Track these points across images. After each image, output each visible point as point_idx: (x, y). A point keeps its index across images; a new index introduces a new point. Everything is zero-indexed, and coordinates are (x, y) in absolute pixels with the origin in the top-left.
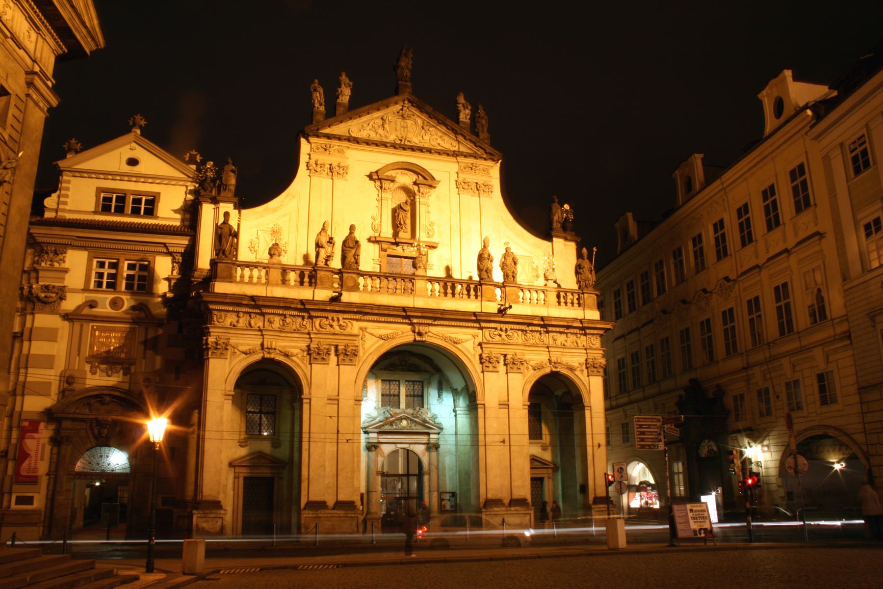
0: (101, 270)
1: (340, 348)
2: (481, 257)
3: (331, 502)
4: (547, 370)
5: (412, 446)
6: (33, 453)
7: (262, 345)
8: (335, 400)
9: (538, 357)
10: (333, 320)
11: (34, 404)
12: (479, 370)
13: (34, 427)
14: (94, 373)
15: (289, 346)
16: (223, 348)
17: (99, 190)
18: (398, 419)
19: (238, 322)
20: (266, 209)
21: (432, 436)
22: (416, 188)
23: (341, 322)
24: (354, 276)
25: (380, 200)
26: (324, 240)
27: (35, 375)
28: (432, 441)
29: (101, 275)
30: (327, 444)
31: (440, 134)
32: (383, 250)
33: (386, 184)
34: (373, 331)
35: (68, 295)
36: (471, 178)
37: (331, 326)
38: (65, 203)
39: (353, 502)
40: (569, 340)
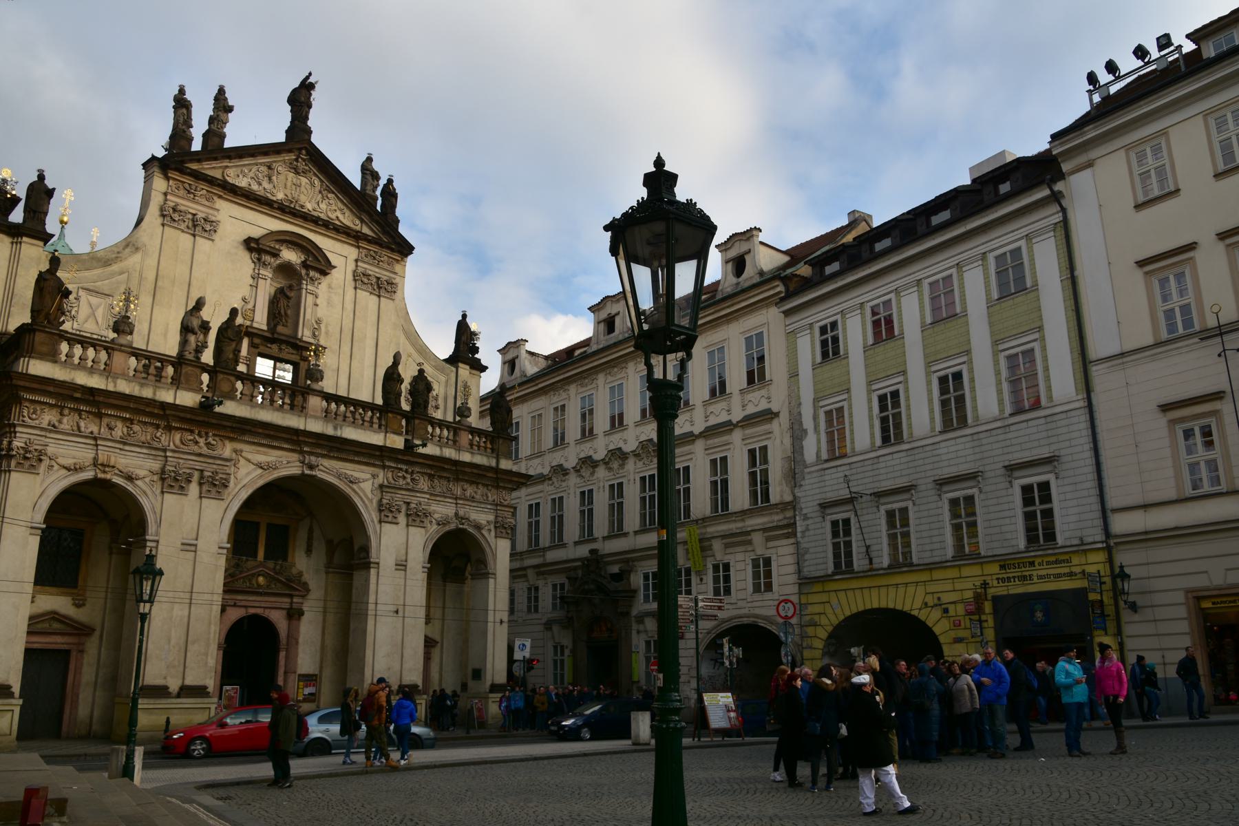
1: (207, 474)
3: (174, 686)
5: (267, 611)
7: (95, 459)
8: (190, 547)
9: (443, 509)
10: (200, 435)
12: (376, 521)
15: (134, 464)
16: (32, 460)
18: (253, 575)
19: (60, 422)
20: (92, 258)
21: (295, 600)
22: (304, 272)
23: (210, 439)
24: (232, 378)
26: (195, 323)
28: (295, 606)
30: (176, 607)
31: (340, 205)
33: (267, 258)
34: (249, 456)
36: (373, 270)
37: (197, 443)
39: (205, 688)
40: (479, 492)
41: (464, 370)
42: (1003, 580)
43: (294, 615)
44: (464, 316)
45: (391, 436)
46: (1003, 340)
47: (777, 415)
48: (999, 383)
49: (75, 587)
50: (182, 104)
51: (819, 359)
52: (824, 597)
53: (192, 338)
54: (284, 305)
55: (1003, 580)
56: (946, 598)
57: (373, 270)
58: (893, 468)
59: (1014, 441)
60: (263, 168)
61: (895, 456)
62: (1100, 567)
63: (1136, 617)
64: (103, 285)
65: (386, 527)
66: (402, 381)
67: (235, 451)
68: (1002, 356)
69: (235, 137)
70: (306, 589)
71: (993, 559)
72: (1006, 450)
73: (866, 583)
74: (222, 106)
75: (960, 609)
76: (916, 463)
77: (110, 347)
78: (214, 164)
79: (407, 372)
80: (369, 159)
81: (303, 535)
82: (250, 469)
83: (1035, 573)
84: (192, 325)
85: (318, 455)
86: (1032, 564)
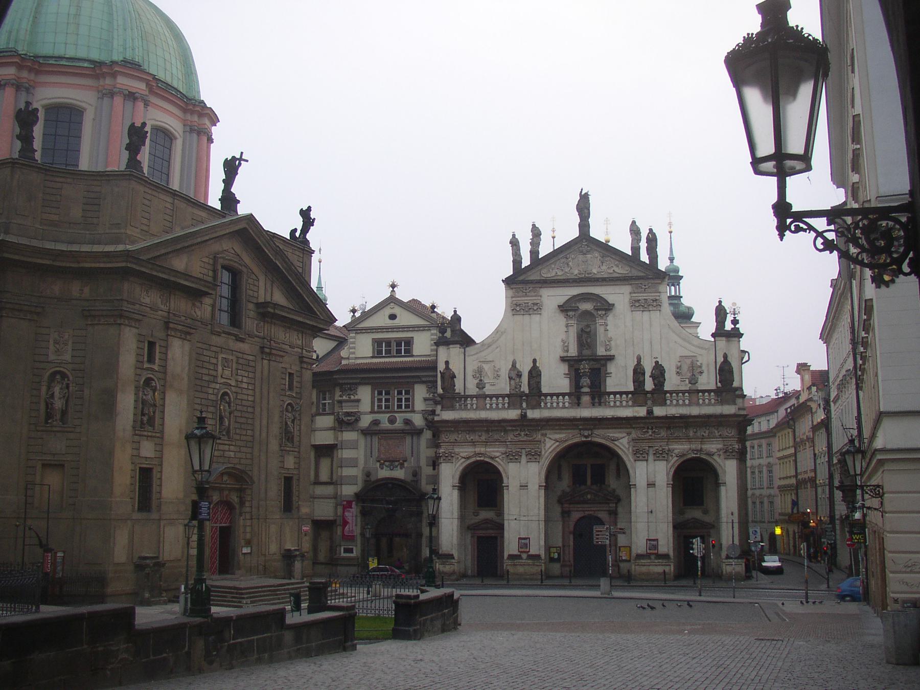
0: (380, 397)
2: (635, 371)
4: (689, 456)
6: (350, 521)
9: (680, 448)
11: (349, 491)
13: (349, 505)
14: (382, 468)
16: (449, 457)
17: (374, 341)
25: (567, 326)
27: (347, 472)
29: (380, 400)
32: (570, 366)
33: (570, 313)
35: (362, 416)
36: (641, 296)
38: (354, 353)
41: (722, 343)
43: (614, 513)
44: (720, 302)
45: (637, 408)
49: (496, 506)
50: (514, 243)
53: (513, 382)
54: (586, 338)
57: (641, 296)
60: (563, 260)
64: (489, 358)
65: (639, 463)
66: (644, 374)
67: (542, 435)
69: (545, 250)
70: (619, 500)
74: (536, 233)
77: (477, 397)
78: (534, 271)
79: (648, 368)
80: (634, 223)
81: (613, 467)
82: (551, 444)
84: (515, 374)
85: (588, 430)
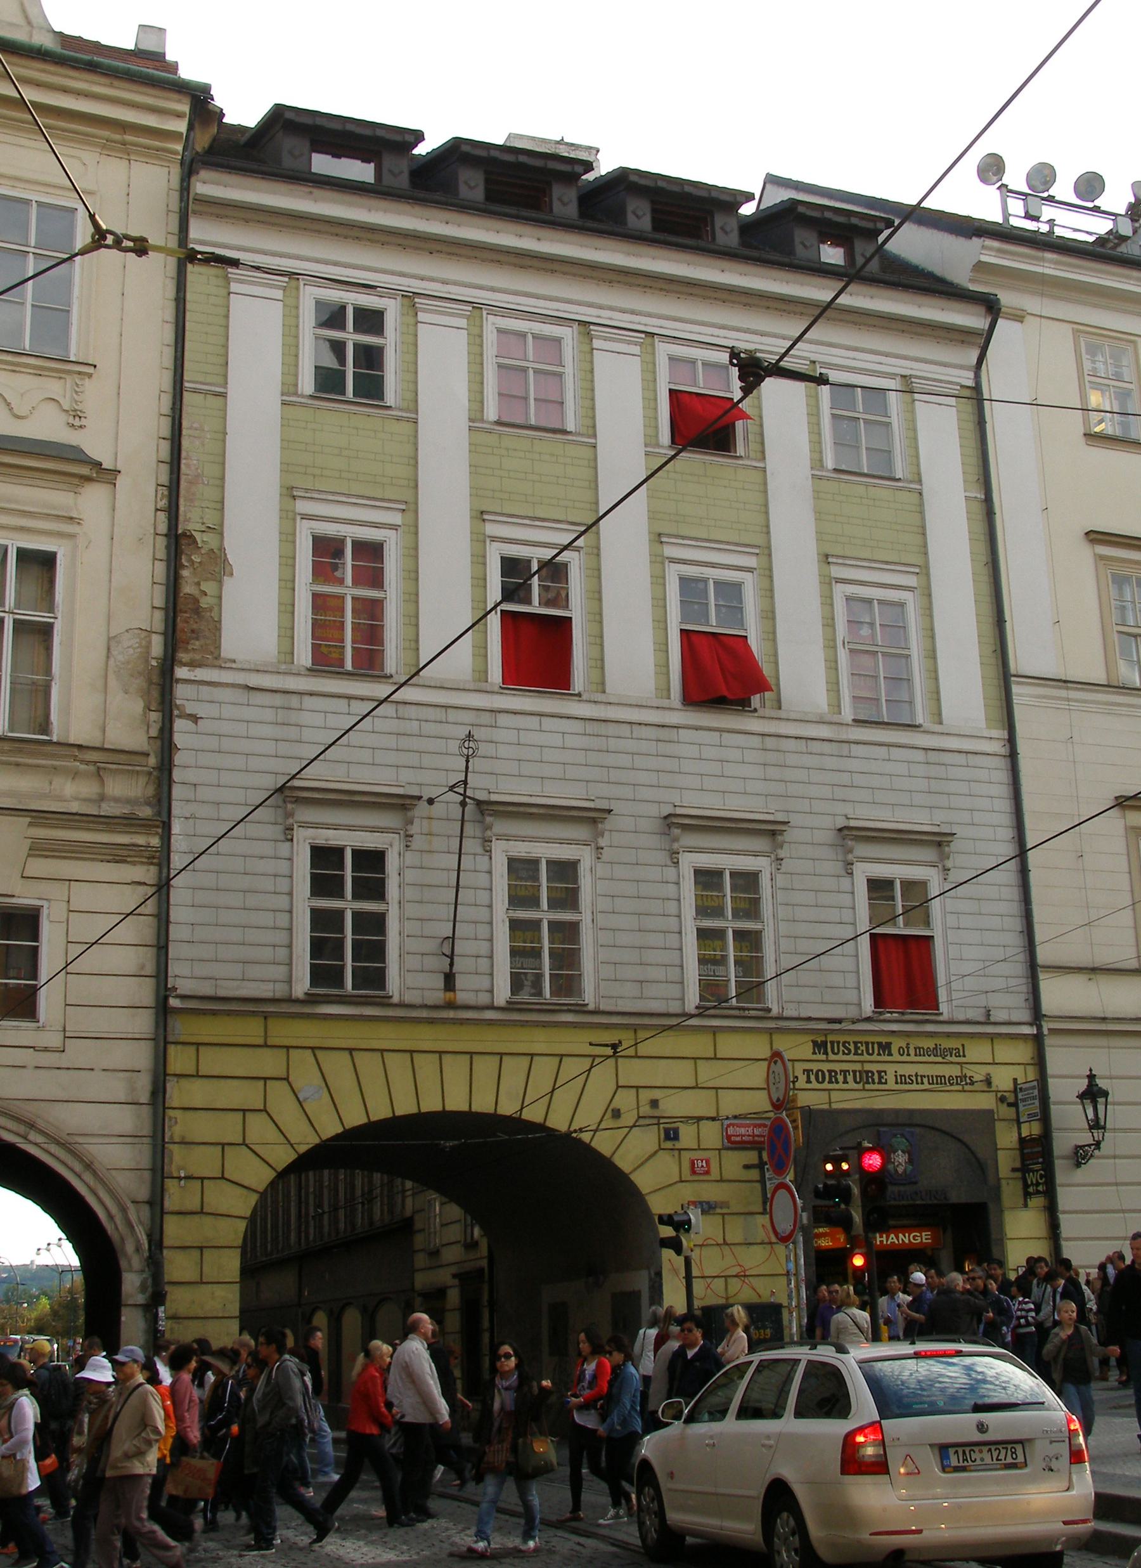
42: (820, 1076)
46: (844, 559)
47: (102, 474)
48: (830, 645)
51: (307, 383)
52: (269, 1063)
55: (820, 1076)
56: (674, 1105)
58: (535, 746)
59: (859, 780)
61: (548, 723)
62: (1018, 1073)
63: (1080, 1175)
68: (673, 574)
71: (800, 1025)
72: (840, 793)
73: (426, 1038)
75: (711, 1134)
76: (611, 759)
83: (890, 1069)
86: (886, 1048)
